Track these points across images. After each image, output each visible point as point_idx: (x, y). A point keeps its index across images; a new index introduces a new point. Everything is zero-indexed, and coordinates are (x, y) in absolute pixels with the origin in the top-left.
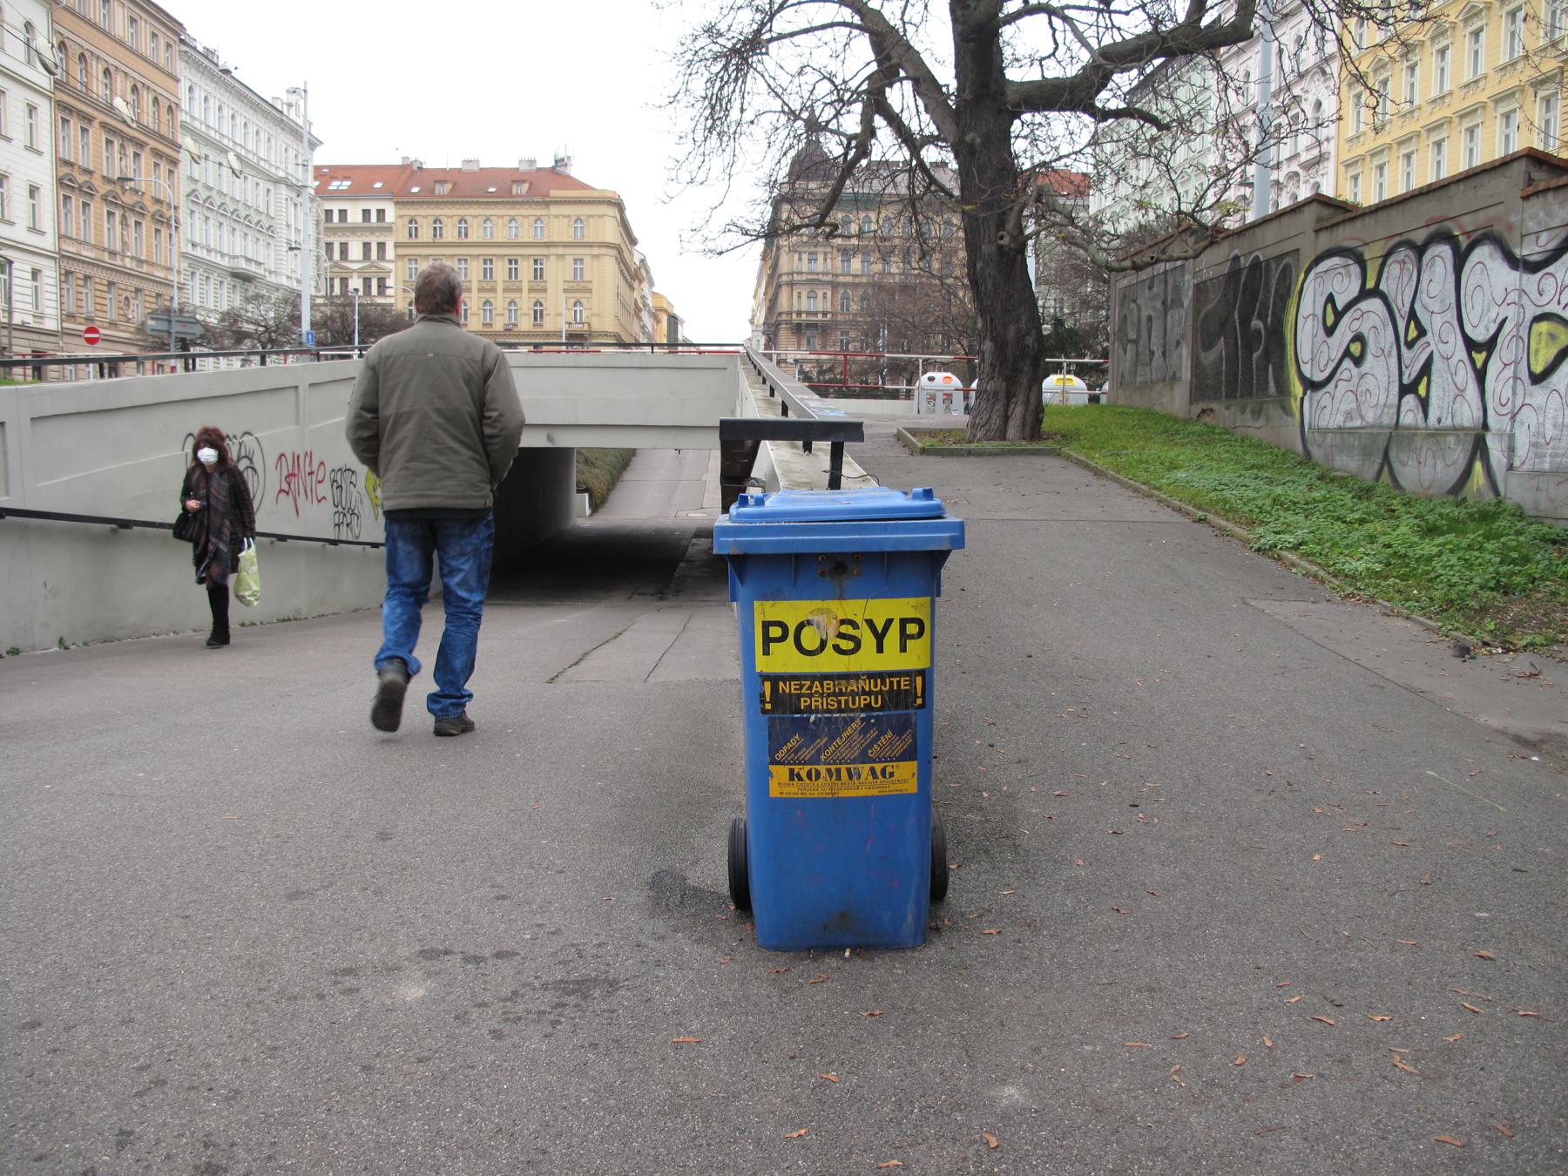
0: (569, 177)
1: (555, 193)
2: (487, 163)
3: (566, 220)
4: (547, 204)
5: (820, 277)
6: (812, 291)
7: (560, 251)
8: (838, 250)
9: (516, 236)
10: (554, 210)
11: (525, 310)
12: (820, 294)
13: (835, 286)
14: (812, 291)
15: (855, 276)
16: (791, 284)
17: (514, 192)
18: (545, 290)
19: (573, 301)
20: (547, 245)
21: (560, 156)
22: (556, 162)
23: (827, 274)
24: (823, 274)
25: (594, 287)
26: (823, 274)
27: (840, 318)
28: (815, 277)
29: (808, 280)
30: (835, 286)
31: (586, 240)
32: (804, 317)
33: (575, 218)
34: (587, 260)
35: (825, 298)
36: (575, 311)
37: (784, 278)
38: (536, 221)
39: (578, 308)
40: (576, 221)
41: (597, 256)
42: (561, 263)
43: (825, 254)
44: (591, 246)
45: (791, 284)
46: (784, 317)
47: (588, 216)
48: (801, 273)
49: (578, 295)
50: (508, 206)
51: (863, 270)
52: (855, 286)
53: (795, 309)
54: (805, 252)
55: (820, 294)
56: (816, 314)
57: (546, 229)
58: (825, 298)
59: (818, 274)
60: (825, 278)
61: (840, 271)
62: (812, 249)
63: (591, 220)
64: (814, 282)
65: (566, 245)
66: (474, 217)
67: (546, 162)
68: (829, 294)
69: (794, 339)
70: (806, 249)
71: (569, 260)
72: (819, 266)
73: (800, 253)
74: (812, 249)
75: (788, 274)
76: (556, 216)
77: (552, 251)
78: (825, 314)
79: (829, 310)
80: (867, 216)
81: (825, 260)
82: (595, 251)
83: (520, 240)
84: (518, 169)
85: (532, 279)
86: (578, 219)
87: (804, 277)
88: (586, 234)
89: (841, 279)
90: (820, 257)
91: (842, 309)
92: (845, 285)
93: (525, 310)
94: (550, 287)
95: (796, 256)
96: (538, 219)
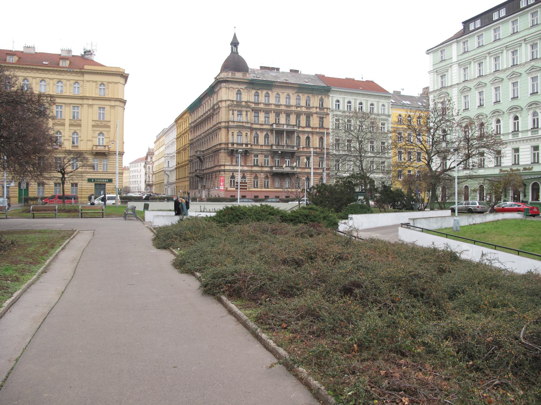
0: (92, 61)
1: (87, 67)
2: (40, 49)
3: (94, 84)
4: (83, 73)
5: (244, 124)
6: (240, 132)
7: (90, 102)
8: (252, 110)
9: (62, 91)
10: (87, 77)
11: (67, 137)
12: (244, 134)
13: (252, 129)
14: (240, 132)
15: (262, 125)
16: (227, 128)
17: (61, 65)
18: (80, 125)
19: (97, 133)
20: (82, 98)
21: (88, 49)
22: (85, 52)
23: (248, 123)
24: (246, 123)
25: (112, 124)
26: (246, 123)
27: (254, 147)
28: (241, 124)
29: (237, 126)
30: (252, 129)
31: (107, 96)
32: (235, 146)
33: (100, 83)
34: (107, 108)
35: (246, 136)
36: (99, 139)
37: (223, 124)
38: (75, 83)
39: (101, 137)
40: (101, 84)
41: (114, 106)
42: (90, 109)
43: (247, 112)
44: (110, 100)
45: (227, 128)
46: (223, 146)
47: (108, 82)
48: (234, 122)
49: (101, 129)
50: (57, 73)
51: (265, 121)
52: (262, 130)
53: (231, 141)
54: (236, 110)
55: (244, 134)
56: (242, 144)
57: (81, 89)
58: (246, 136)
59: (243, 122)
60: (247, 125)
61: (253, 122)
62: (240, 109)
63: (110, 85)
64: (240, 127)
65: (94, 99)
66: (34, 78)
67: (78, 52)
68: (249, 134)
69: (229, 159)
70: (236, 108)
71: (96, 108)
72: (243, 118)
73: (233, 110)
74: (240, 109)
75: (225, 122)
76: (88, 81)
77: (85, 102)
78: (247, 145)
79: (249, 143)
80: (267, 93)
81: (247, 115)
82: (113, 103)
83: (64, 94)
84: (60, 55)
85: (72, 118)
86: (102, 84)
87: (236, 124)
88: (107, 93)
89: (255, 126)
90: (244, 113)
91: (254, 143)
92: (256, 129)
93: (67, 137)
94: (83, 123)
95: (231, 112)
96: (76, 82)
